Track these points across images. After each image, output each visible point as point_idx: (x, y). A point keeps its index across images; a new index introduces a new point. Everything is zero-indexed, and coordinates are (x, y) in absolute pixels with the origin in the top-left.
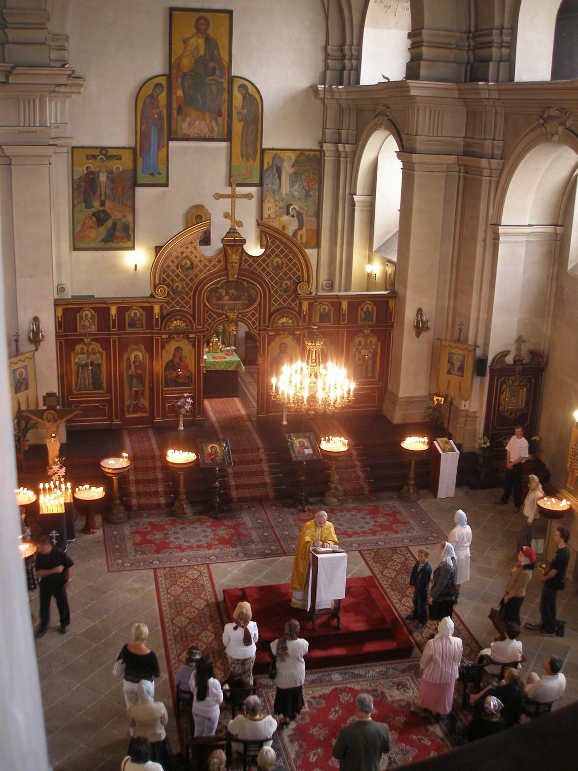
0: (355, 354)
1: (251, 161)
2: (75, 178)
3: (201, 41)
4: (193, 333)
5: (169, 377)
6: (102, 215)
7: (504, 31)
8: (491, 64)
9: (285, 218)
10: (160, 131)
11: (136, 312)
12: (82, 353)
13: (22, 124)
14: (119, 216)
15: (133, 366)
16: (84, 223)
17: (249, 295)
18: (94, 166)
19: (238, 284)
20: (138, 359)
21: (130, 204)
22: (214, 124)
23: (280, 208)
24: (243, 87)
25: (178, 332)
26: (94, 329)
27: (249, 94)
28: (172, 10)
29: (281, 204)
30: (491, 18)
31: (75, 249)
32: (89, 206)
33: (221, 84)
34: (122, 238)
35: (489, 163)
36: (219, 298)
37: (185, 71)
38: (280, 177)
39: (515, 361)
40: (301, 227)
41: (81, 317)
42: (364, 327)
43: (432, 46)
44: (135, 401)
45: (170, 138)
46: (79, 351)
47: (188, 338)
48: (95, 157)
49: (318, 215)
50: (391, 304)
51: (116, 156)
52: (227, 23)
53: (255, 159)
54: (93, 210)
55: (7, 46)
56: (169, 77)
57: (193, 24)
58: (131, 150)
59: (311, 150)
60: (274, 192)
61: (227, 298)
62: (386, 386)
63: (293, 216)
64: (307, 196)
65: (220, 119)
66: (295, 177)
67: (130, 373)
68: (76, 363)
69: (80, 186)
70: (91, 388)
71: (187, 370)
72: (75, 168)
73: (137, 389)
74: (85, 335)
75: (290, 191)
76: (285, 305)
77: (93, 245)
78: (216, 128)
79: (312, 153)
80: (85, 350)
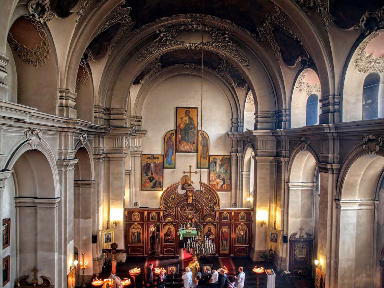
1: (205, 160)
2: (143, 165)
3: (187, 119)
4: (174, 222)
6: (152, 178)
7: (287, 110)
8: (282, 122)
9: (218, 180)
10: (173, 149)
11: (154, 214)
12: (134, 228)
13: (115, 147)
14: (158, 179)
16: (145, 181)
17: (196, 209)
18: (149, 161)
19: (192, 205)
21: (162, 175)
22: (192, 147)
23: (216, 176)
24: (202, 134)
25: (169, 222)
26: (138, 219)
27: (205, 136)
28: (177, 108)
29: (217, 175)
30: (282, 106)
31: (142, 190)
32: (147, 175)
33: (194, 133)
34: (158, 187)
35: (284, 159)
36: (185, 210)
37: (182, 128)
38: (216, 166)
39: (300, 237)
40: (224, 183)
41: (134, 215)
42: (241, 222)
43: (262, 117)
45: (176, 152)
47: (173, 224)
48: (150, 158)
49: (230, 179)
50: (252, 213)
51: (157, 158)
52: (196, 112)
53: (207, 159)
54: (149, 176)
55: (110, 121)
56: (176, 130)
57: (185, 113)
58: (162, 156)
59: (227, 156)
60: (214, 171)
61: (188, 210)
62: (251, 246)
63: (221, 180)
64: (226, 172)
65: (194, 145)
66: (222, 165)
68: (131, 232)
69: (144, 168)
70: (137, 242)
72: (143, 162)
74: (135, 222)
75: (220, 171)
76: (210, 213)
77: (148, 189)
78: (192, 148)
79: (228, 157)
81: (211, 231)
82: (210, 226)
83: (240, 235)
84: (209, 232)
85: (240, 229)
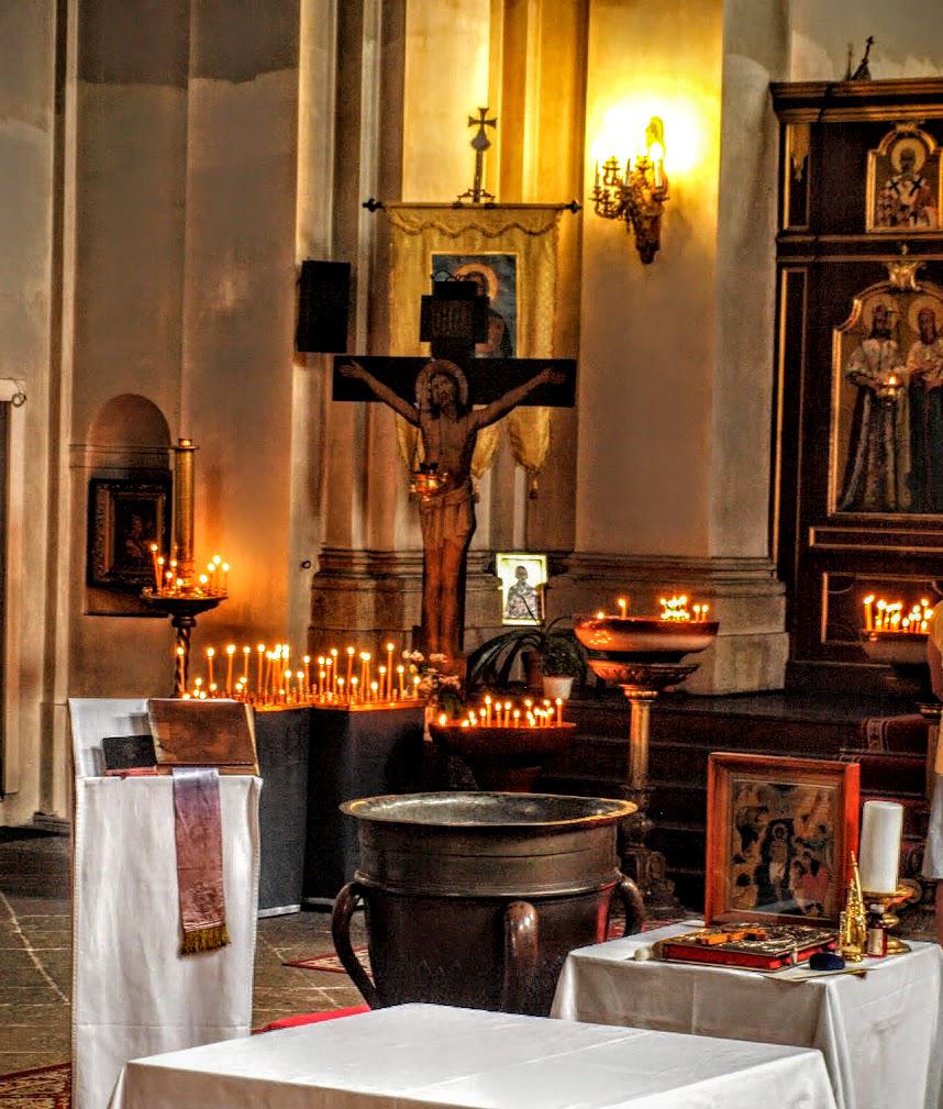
12: (880, 333)
70: (906, 499)
74: (890, 247)
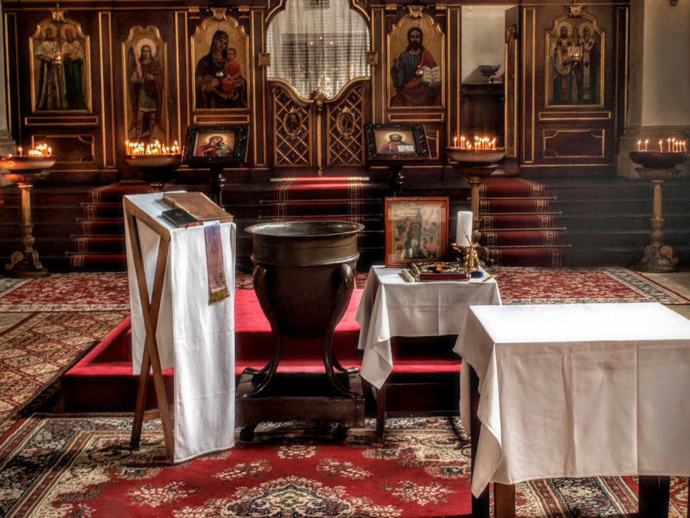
0: (556, 55)
5: (203, 88)
15: (139, 65)
20: (148, 56)
44: (143, 132)
46: (44, 35)
67: (134, 78)
70: (65, 104)
71: (236, 76)
73: (146, 110)
80: (54, 34)
81: (422, 48)
82: (415, 24)
83: (565, 64)
84: (412, 52)
85: (564, 36)
